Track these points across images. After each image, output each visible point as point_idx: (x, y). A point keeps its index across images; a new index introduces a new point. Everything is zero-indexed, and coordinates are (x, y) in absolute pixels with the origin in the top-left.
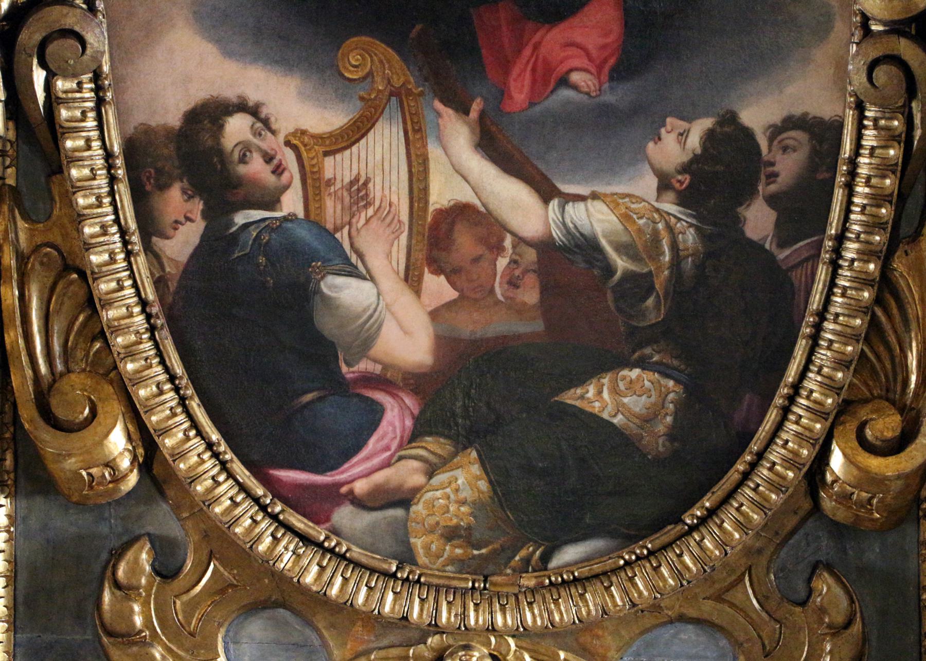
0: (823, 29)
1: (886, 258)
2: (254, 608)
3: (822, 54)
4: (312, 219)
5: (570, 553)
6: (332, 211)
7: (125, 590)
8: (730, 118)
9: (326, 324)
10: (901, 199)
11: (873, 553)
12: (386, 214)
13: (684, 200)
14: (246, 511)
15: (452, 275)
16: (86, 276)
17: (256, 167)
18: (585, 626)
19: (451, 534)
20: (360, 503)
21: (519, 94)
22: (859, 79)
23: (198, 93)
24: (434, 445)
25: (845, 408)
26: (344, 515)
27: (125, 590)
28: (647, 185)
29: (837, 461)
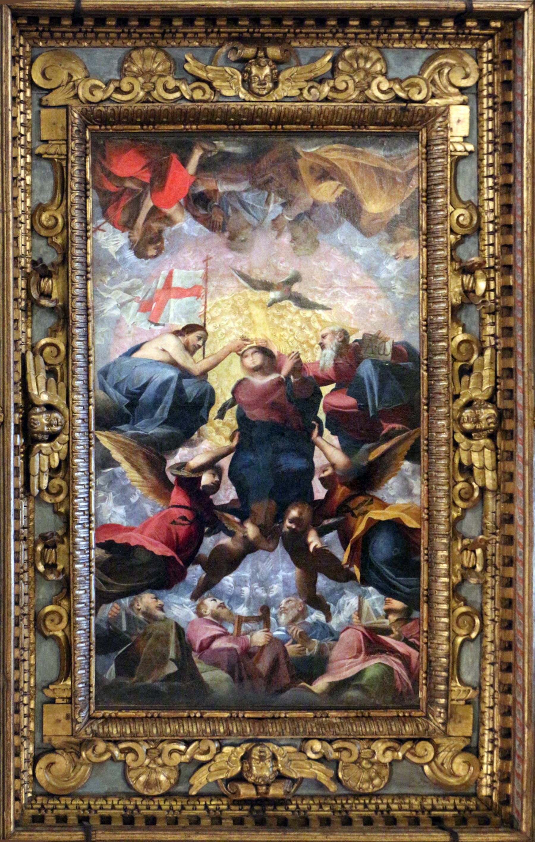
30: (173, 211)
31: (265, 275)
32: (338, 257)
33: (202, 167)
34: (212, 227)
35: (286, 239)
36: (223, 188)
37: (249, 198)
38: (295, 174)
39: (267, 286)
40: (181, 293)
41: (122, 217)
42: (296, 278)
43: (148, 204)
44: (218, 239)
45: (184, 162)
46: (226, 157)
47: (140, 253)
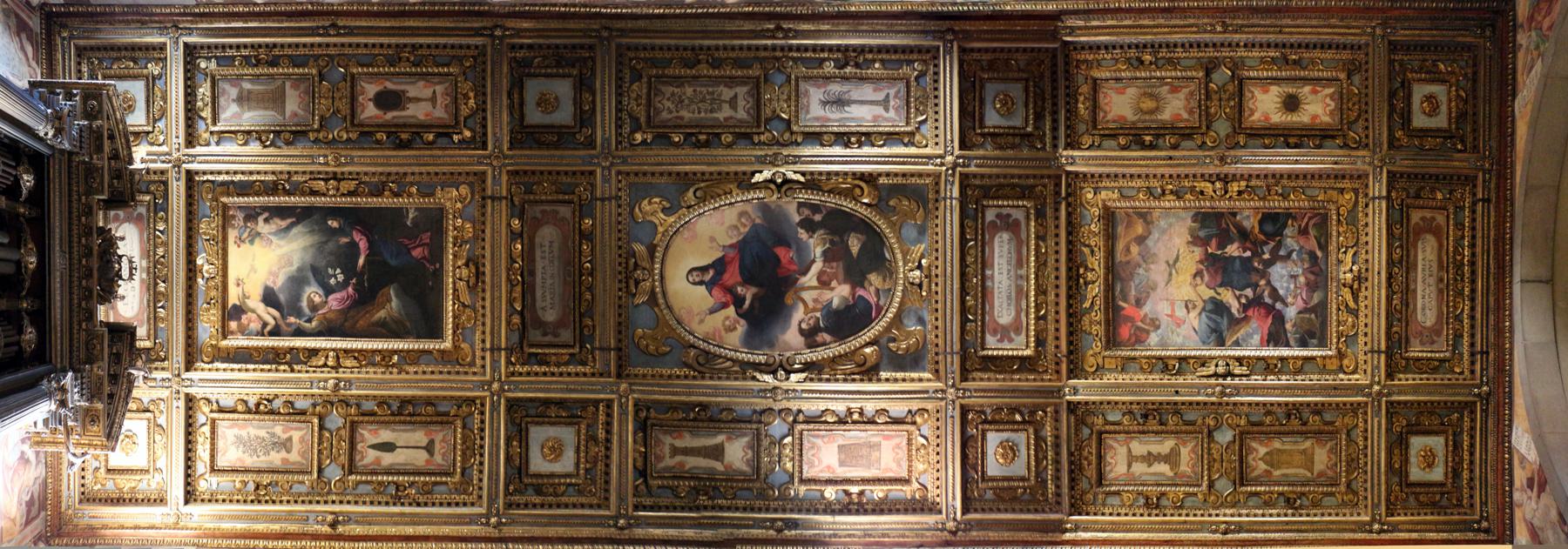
0: (780, 206)
1: (824, 192)
2: (901, 322)
3: (785, 206)
4: (822, 310)
5: (887, 255)
6: (819, 306)
7: (898, 349)
8: (798, 224)
9: (843, 307)
10: (812, 189)
11: (884, 194)
12: (820, 295)
13: (814, 232)
14: (882, 323)
15: (831, 280)
16: (835, 357)
17: (811, 322)
18: (902, 252)
19: (884, 280)
20: (879, 299)
21: (794, 267)
22: (788, 199)
23: (798, 334)
24: (866, 284)
25: (855, 199)
26: (881, 303)
27: (898, 349)
28: (811, 241)
29: (866, 201)
30: (1142, 314)
31: (1166, 275)
32: (1160, 244)
33: (1125, 301)
34: (1148, 297)
35: (1152, 266)
36: (1133, 293)
37: (1137, 282)
38: (1128, 262)
39: (1170, 274)
40: (1173, 310)
41: (1144, 335)
42: (1167, 262)
43: (1140, 324)
44: (1152, 295)
45: (1123, 309)
46: (1122, 290)
47: (1158, 327)
